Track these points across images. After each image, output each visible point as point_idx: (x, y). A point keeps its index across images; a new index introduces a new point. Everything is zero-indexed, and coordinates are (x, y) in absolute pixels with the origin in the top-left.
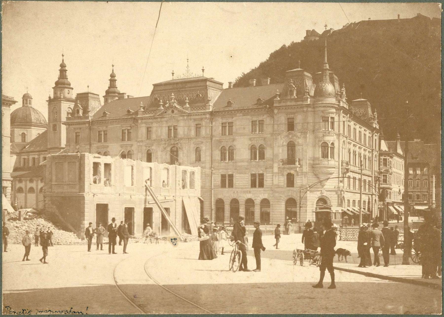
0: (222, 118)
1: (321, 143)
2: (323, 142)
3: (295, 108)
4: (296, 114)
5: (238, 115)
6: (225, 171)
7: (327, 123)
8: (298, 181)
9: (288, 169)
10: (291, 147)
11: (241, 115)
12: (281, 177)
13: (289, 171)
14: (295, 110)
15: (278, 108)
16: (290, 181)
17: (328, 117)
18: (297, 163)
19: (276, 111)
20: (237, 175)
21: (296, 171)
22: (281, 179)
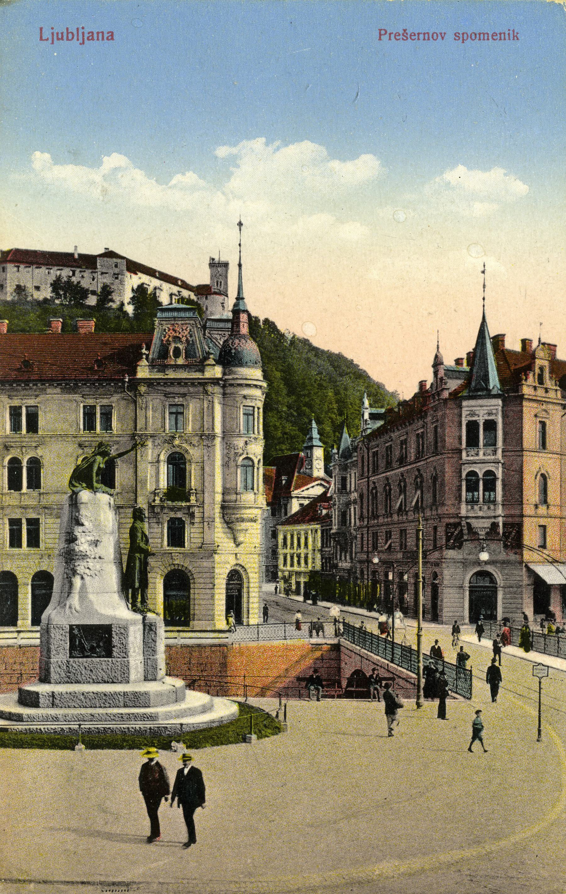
0: (10, 397)
1: (241, 458)
2: (244, 456)
3: (165, 383)
4: (188, 398)
5: (49, 391)
6: (18, 511)
7: (251, 418)
8: (192, 534)
9: (172, 509)
10: (178, 463)
11: (58, 390)
12: (156, 526)
13: (172, 515)
14: (186, 389)
15: (149, 382)
16: (176, 536)
17: (254, 407)
18: (193, 498)
19: (143, 389)
20: (48, 521)
21: (192, 515)
22: (156, 530)
